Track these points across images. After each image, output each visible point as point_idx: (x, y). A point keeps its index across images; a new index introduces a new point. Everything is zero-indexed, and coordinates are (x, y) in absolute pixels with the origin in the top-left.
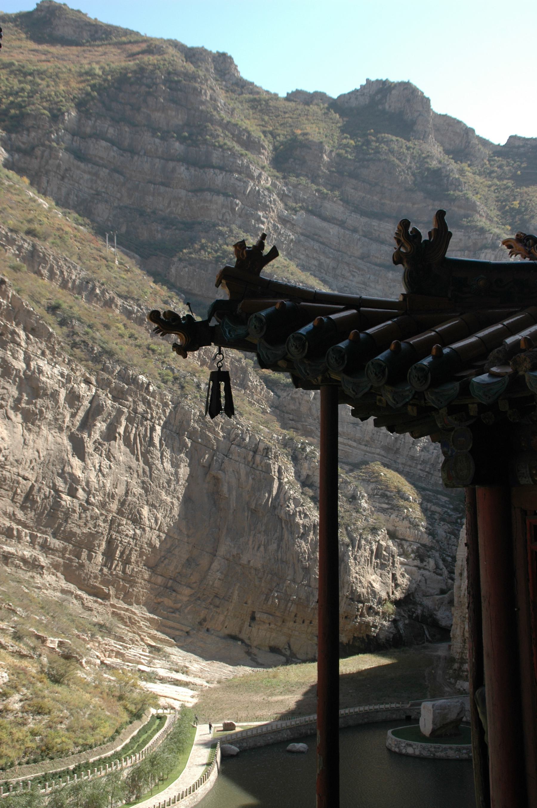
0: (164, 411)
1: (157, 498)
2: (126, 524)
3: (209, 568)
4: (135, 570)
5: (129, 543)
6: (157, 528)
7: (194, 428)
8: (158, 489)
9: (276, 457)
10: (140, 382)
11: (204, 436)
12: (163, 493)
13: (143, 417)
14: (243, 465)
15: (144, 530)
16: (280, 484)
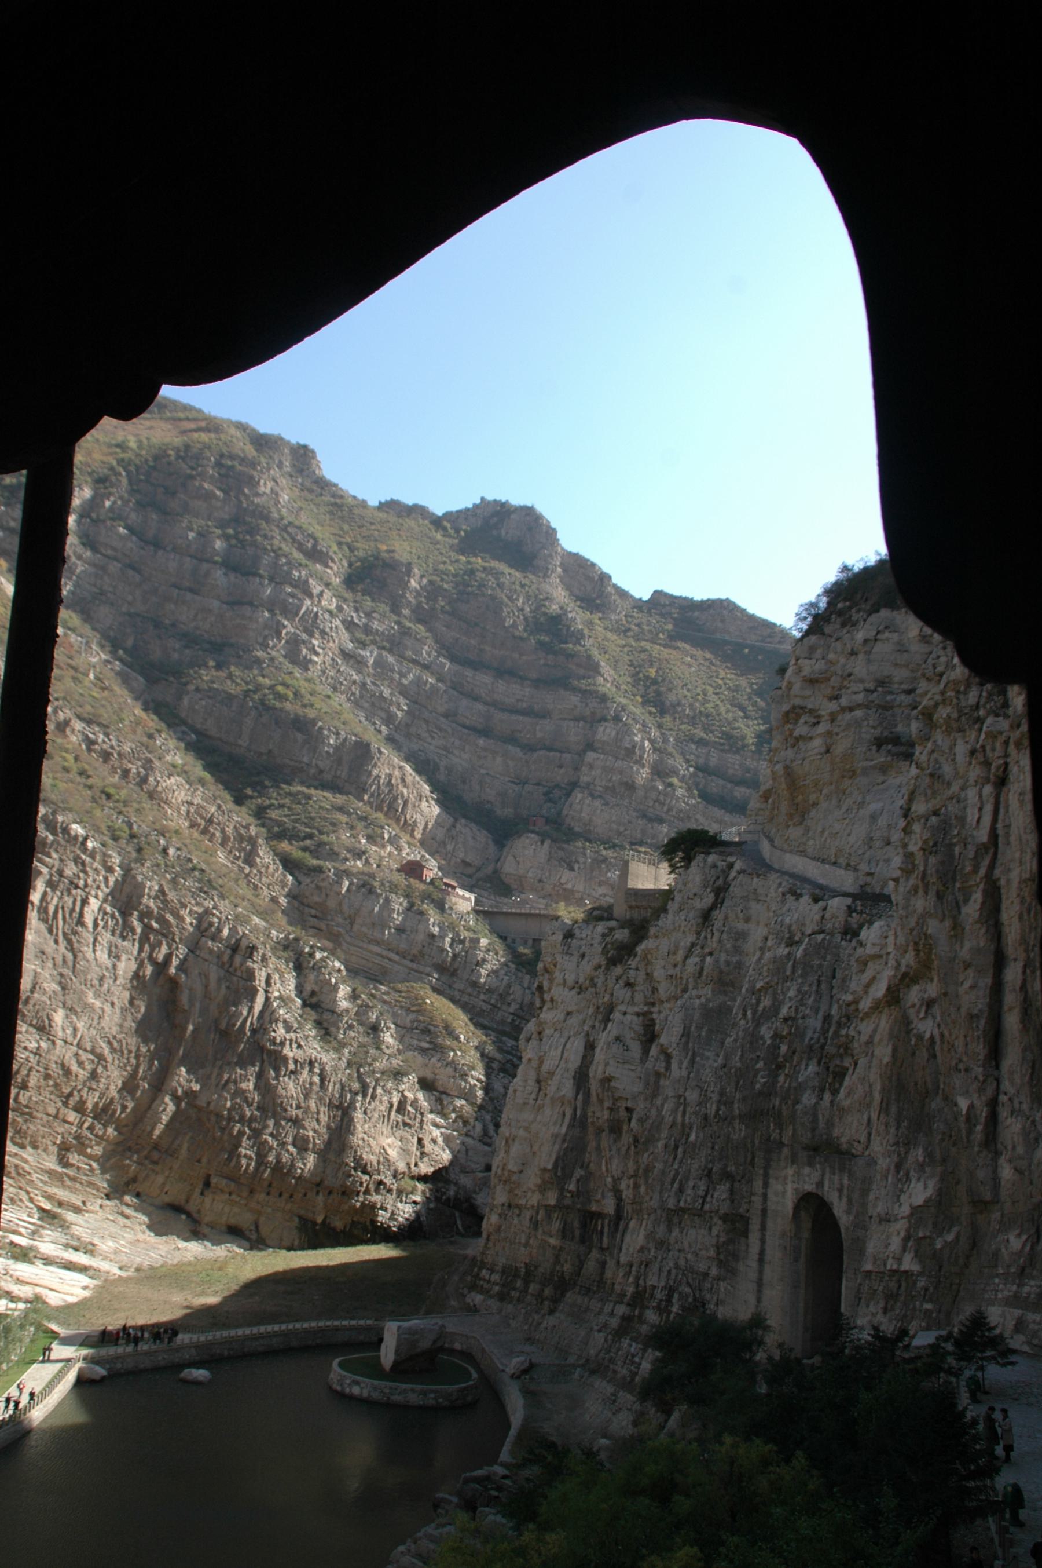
0: (106, 879)
1: (80, 999)
2: (27, 1032)
3: (149, 1107)
4: (34, 1099)
5: (27, 1060)
6: (75, 1043)
7: (148, 907)
8: (83, 987)
9: (264, 959)
10: (73, 833)
11: (161, 920)
12: (90, 994)
13: (72, 883)
14: (215, 968)
15: (54, 1043)
16: (267, 999)
